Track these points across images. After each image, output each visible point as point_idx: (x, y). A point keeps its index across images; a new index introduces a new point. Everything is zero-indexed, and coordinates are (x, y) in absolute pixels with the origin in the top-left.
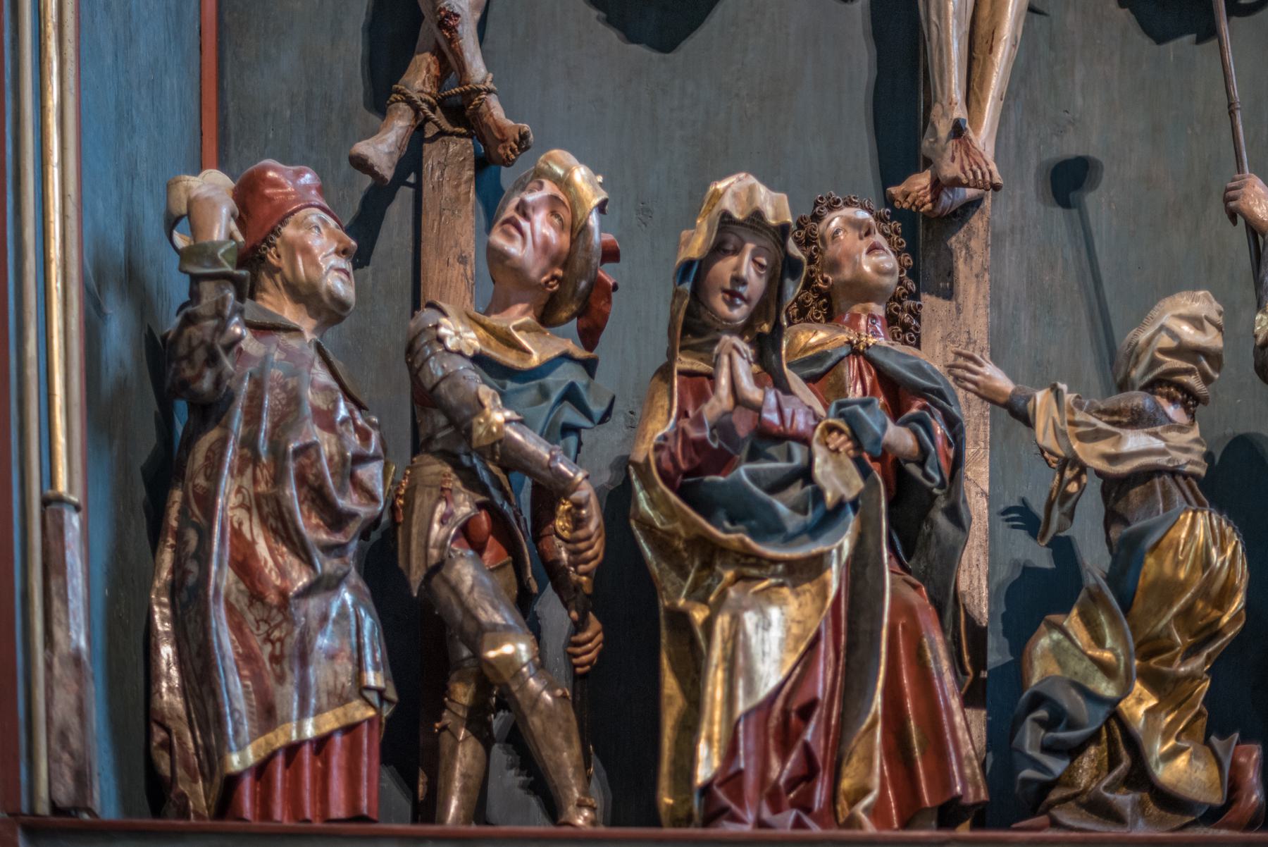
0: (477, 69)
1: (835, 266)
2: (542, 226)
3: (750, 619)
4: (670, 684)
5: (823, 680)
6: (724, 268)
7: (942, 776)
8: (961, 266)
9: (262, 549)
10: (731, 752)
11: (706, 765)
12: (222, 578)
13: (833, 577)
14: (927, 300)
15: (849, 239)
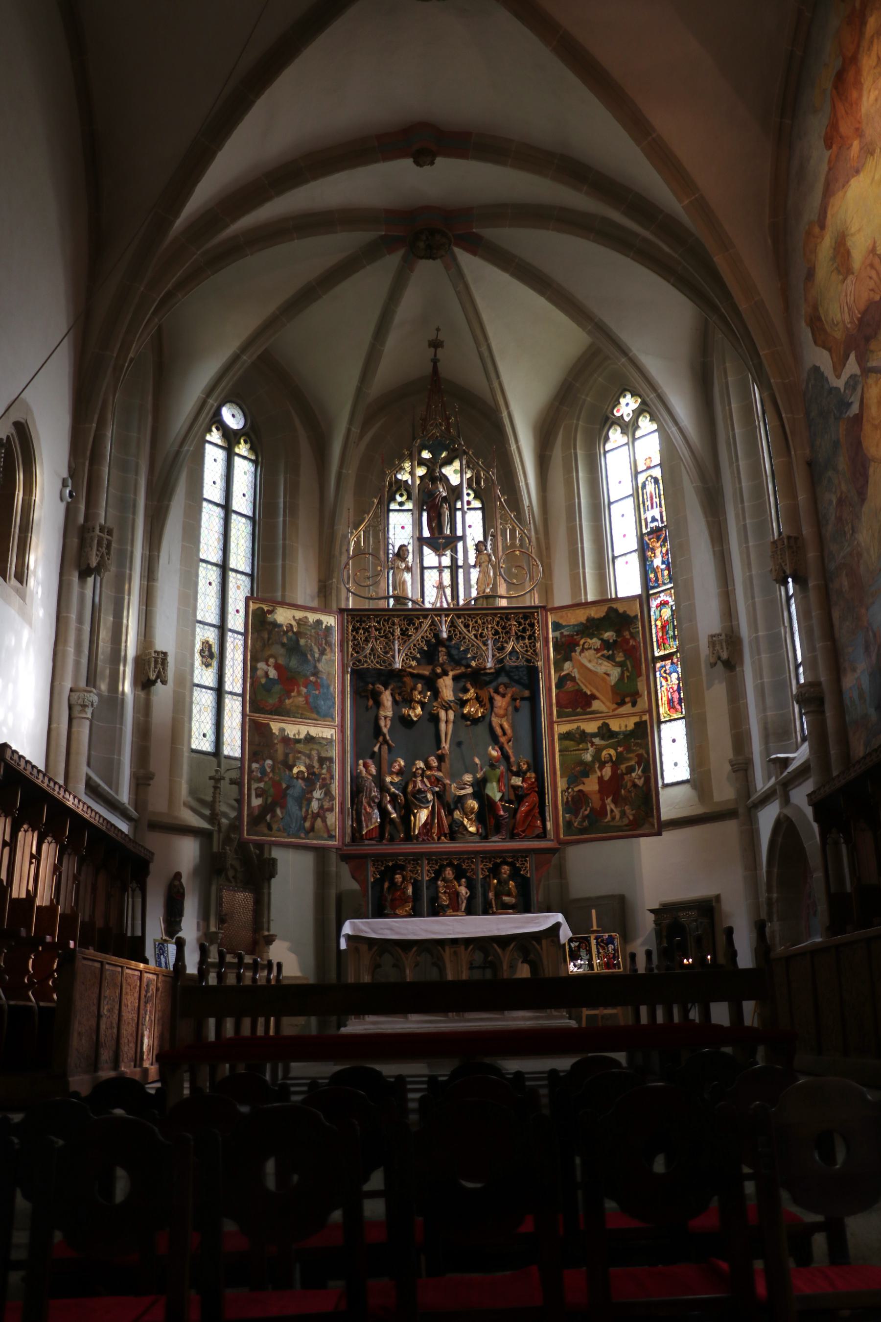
0: (388, 738)
1: (430, 764)
2: (397, 767)
3: (421, 814)
4: (412, 818)
5: (429, 821)
6: (418, 771)
7: (444, 831)
8: (446, 760)
9: (367, 807)
10: (419, 830)
11: (417, 832)
12: (363, 811)
13: (430, 808)
14: (442, 764)
15: (432, 762)
